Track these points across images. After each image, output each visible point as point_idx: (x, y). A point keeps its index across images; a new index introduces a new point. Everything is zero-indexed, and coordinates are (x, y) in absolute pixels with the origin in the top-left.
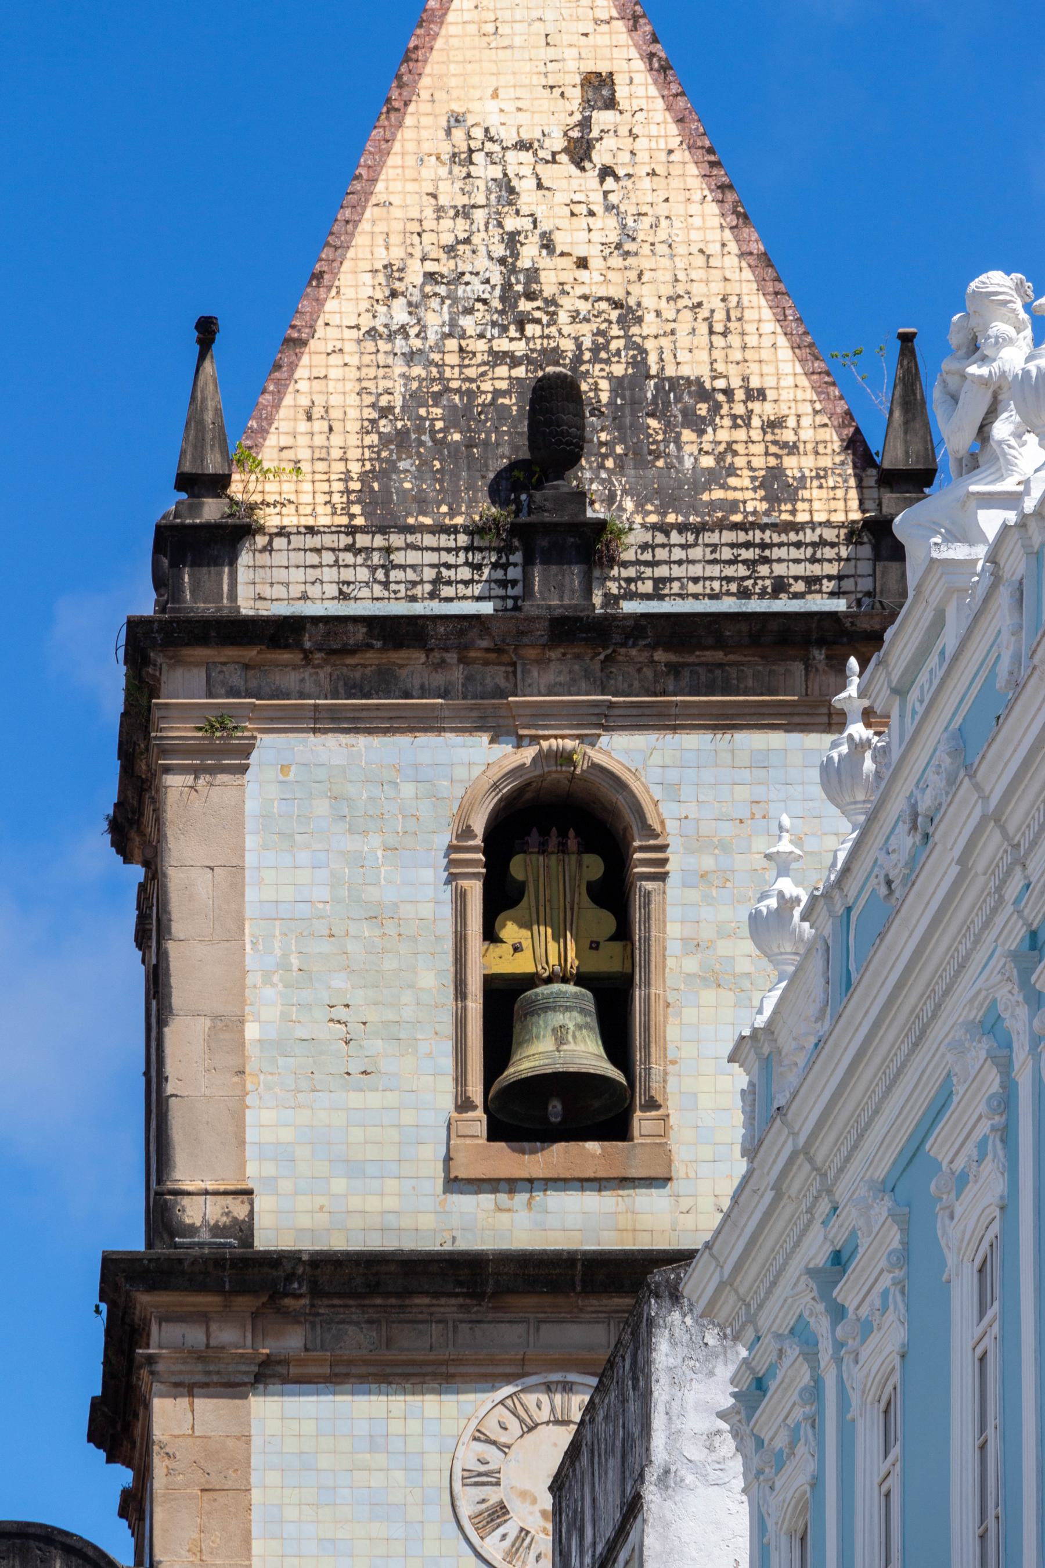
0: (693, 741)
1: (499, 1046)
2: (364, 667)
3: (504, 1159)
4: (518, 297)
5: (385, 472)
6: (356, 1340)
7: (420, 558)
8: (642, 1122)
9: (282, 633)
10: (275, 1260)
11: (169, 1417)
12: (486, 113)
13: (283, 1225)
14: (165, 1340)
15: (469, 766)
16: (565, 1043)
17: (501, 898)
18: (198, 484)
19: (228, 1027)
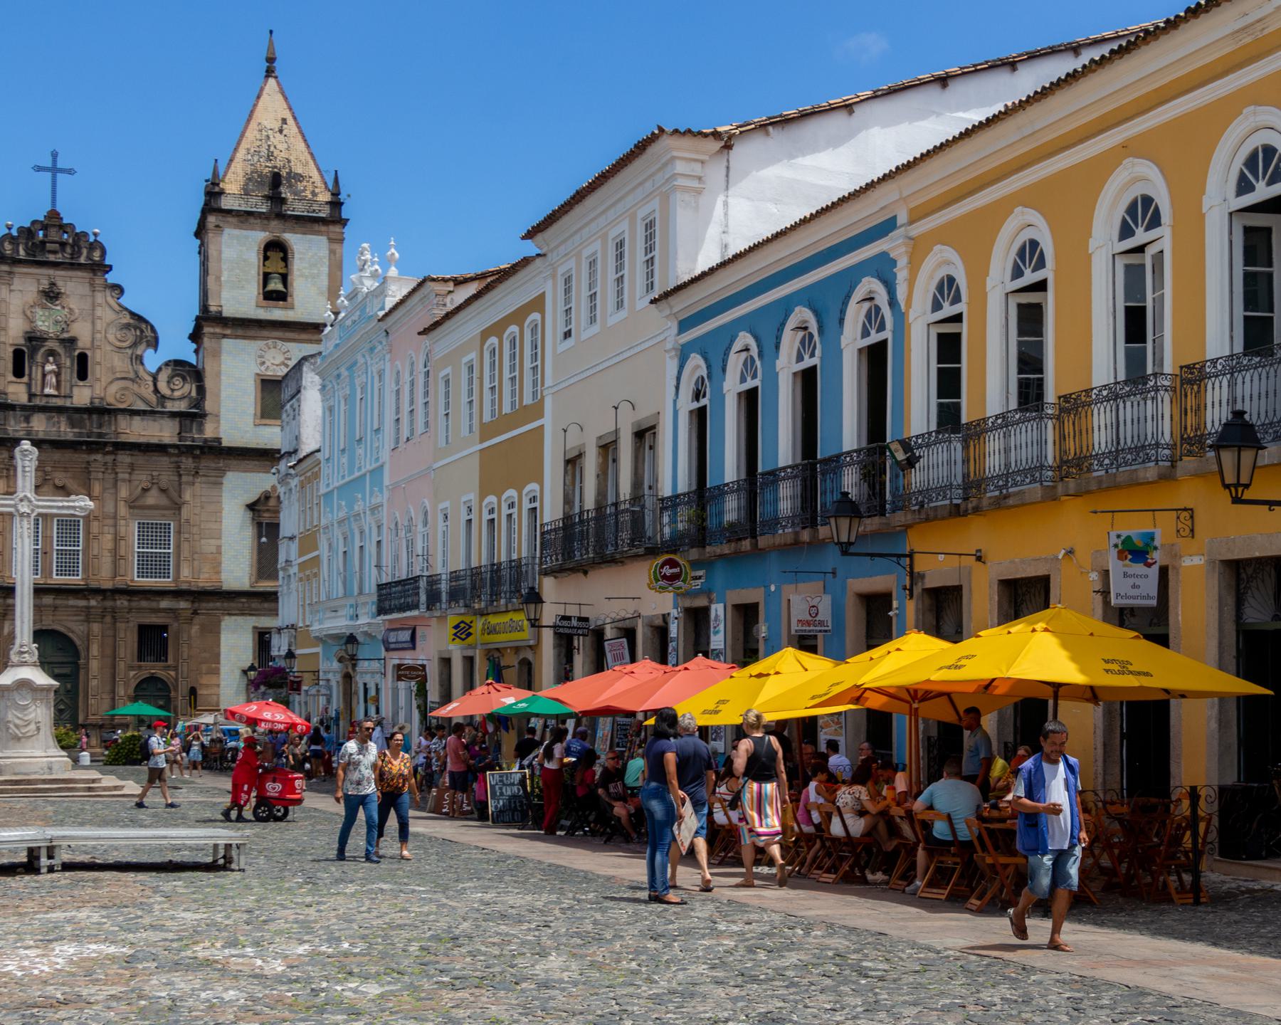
0: (299, 236)
1: (265, 283)
2: (244, 217)
3: (265, 303)
4: (270, 156)
5: (246, 184)
6: (240, 332)
7: (253, 201)
8: (289, 299)
9: (229, 212)
10: (226, 319)
11: (207, 342)
12: (265, 123)
13: (228, 312)
14: (207, 330)
15: (259, 237)
16: (276, 285)
17: (266, 258)
18: (215, 184)
19: (218, 278)
